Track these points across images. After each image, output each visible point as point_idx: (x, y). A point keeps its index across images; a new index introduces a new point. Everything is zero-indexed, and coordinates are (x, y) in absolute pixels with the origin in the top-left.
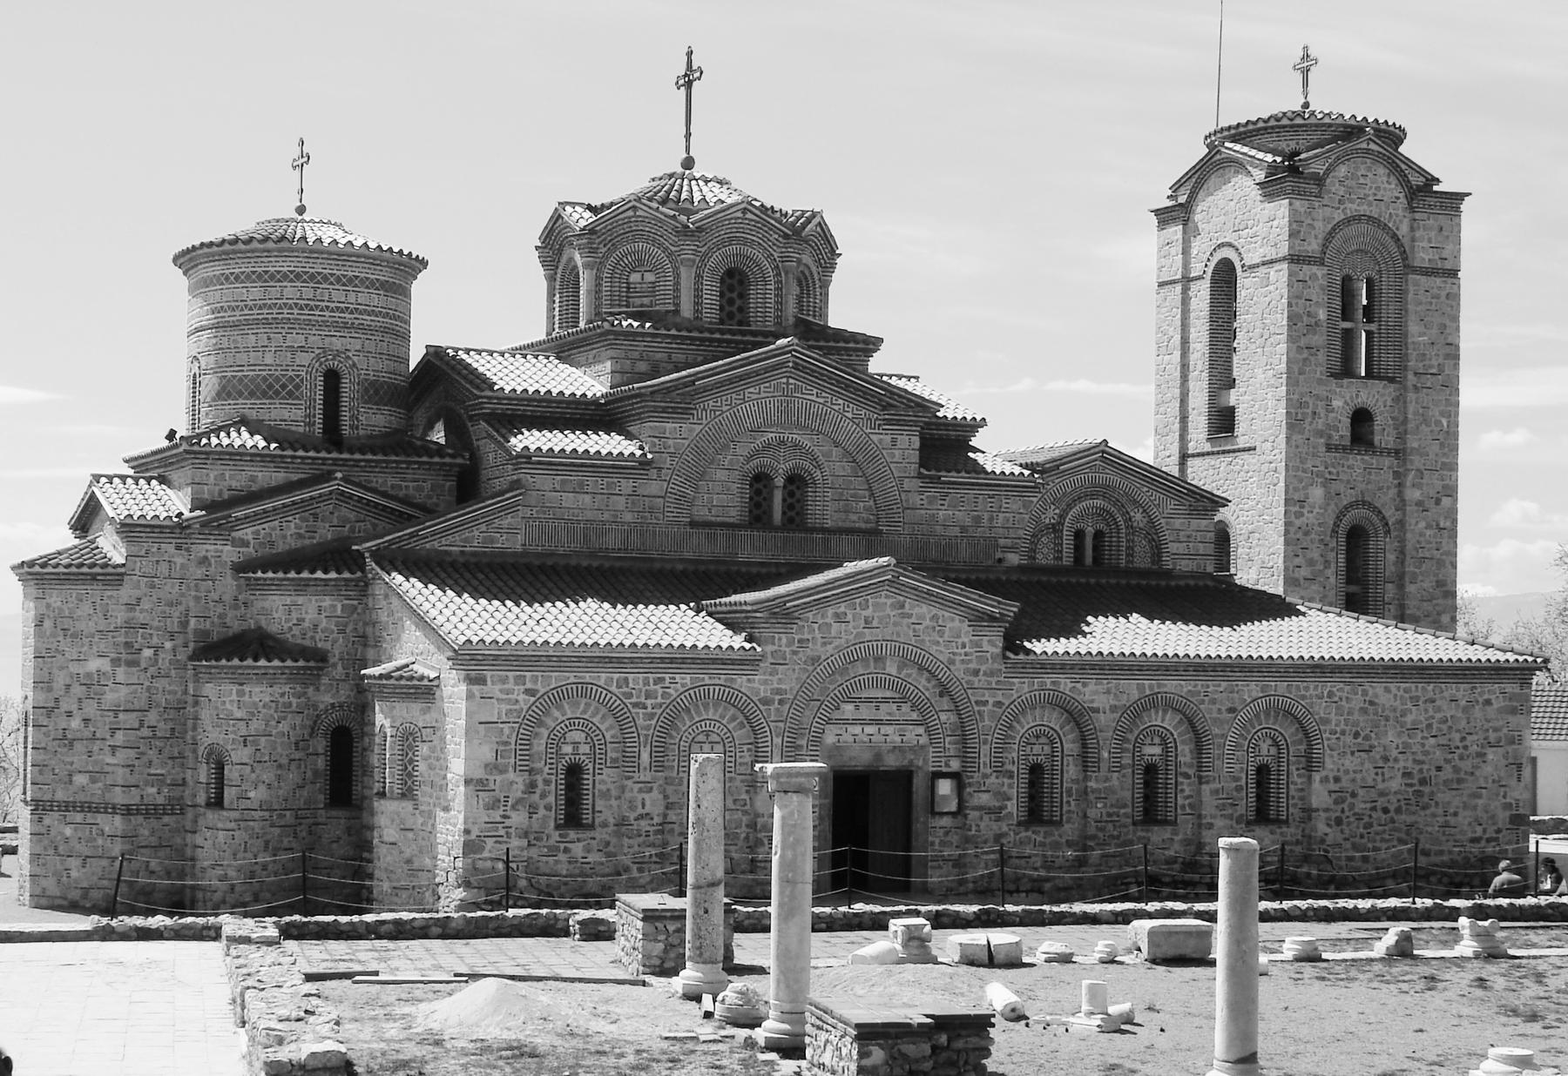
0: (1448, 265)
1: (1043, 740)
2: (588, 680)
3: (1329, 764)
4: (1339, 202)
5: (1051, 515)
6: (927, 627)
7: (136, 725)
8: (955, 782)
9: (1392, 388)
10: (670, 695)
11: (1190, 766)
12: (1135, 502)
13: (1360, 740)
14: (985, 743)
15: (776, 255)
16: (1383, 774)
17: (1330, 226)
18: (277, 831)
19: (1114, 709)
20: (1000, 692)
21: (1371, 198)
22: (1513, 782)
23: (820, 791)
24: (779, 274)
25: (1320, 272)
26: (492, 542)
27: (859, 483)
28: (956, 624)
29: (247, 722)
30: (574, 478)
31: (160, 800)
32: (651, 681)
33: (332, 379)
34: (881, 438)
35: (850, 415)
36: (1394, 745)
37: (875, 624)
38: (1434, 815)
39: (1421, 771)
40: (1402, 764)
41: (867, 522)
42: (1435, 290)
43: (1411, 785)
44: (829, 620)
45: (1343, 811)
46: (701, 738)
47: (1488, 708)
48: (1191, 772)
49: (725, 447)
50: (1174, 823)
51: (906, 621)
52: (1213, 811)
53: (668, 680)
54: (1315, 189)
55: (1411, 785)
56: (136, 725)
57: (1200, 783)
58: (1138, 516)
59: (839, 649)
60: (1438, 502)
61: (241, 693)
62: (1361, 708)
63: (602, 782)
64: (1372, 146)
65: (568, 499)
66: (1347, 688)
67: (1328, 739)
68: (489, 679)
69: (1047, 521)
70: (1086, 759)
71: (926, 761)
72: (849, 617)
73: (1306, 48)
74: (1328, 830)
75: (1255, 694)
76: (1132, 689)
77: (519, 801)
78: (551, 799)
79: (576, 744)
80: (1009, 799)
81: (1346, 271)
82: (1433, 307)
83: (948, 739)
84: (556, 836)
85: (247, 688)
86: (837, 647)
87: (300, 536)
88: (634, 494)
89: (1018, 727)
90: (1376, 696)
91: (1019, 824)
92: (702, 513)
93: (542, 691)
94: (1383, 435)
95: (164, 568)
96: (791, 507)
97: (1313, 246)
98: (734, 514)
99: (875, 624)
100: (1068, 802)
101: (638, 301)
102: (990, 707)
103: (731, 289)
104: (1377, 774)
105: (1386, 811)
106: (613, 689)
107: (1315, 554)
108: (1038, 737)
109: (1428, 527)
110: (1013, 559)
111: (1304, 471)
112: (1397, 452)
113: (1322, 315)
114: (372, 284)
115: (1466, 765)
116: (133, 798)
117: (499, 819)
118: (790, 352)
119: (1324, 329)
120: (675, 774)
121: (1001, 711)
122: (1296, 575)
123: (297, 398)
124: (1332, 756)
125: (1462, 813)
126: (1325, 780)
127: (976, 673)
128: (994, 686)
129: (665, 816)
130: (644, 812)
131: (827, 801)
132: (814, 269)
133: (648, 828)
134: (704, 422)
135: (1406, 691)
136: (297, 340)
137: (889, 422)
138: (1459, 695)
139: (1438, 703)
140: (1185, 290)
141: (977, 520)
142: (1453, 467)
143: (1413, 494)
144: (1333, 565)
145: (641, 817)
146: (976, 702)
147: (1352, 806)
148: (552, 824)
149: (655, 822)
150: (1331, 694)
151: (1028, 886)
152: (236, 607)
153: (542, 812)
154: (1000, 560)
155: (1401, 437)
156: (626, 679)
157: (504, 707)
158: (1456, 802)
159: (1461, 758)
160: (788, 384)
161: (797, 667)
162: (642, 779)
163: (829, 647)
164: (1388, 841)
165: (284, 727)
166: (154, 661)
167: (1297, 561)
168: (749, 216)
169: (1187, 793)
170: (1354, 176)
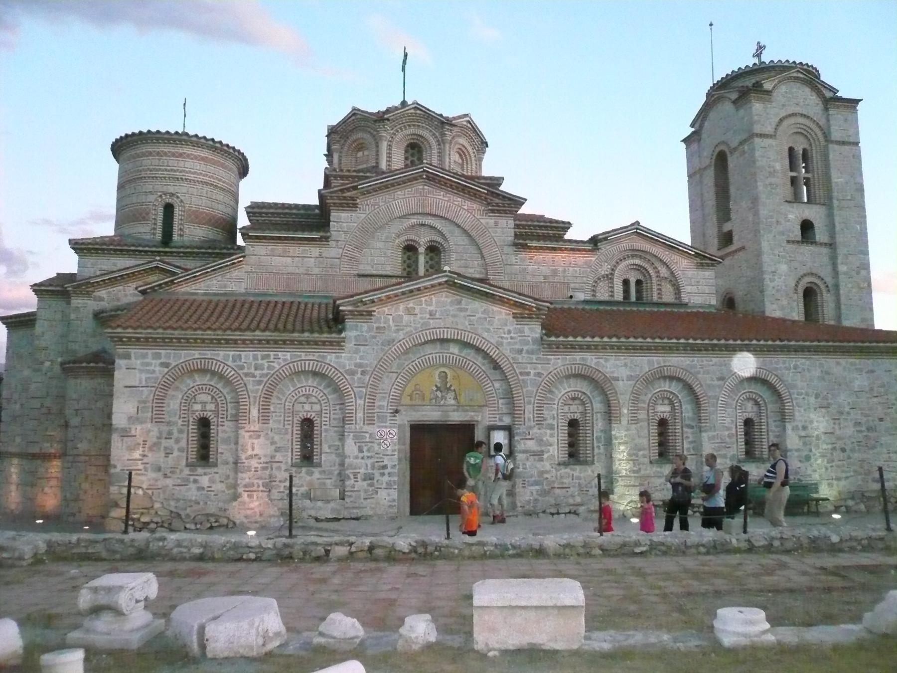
0: (852, 140)
1: (577, 402)
2: (209, 357)
5: (605, 269)
6: (480, 318)
8: (507, 433)
10: (274, 367)
11: (693, 419)
14: (529, 403)
15: (437, 134)
16: (839, 424)
19: (630, 378)
20: (539, 366)
23: (399, 439)
26: (225, 287)
30: (279, 247)
32: (259, 357)
33: (169, 209)
34: (489, 221)
35: (466, 207)
36: (846, 402)
37: (437, 316)
39: (868, 421)
46: (303, 399)
48: (693, 424)
51: (462, 314)
53: (272, 357)
56: (39, 406)
57: (701, 431)
58: (664, 271)
59: (410, 334)
60: (858, 273)
63: (224, 431)
65: (277, 261)
66: (808, 362)
67: (796, 399)
68: (133, 355)
69: (603, 273)
72: (417, 311)
73: (759, 43)
74: (799, 465)
77: (155, 444)
78: (183, 443)
79: (204, 403)
80: (551, 445)
84: (187, 471)
85: (79, 381)
86: (407, 333)
88: (320, 256)
89: (556, 392)
91: (559, 464)
93: (174, 364)
94: (820, 235)
99: (437, 316)
100: (598, 447)
102: (532, 376)
105: (843, 450)
106: (230, 363)
108: (574, 399)
110: (581, 296)
112: (831, 245)
113: (778, 166)
118: (422, 168)
120: (281, 426)
121: (541, 379)
123: (147, 220)
124: (800, 411)
127: (520, 351)
130: (255, 452)
132: (470, 149)
133: (257, 465)
134: (368, 212)
137: (493, 211)
140: (701, 176)
142: (866, 253)
143: (842, 268)
144: (796, 309)
145: (251, 457)
146: (521, 373)
149: (261, 461)
150: (795, 367)
153: (176, 453)
155: (832, 235)
156: (240, 355)
157: (144, 376)
160: (423, 189)
161: (375, 348)
162: (252, 428)
163: (401, 333)
164: (846, 472)
169: (691, 439)
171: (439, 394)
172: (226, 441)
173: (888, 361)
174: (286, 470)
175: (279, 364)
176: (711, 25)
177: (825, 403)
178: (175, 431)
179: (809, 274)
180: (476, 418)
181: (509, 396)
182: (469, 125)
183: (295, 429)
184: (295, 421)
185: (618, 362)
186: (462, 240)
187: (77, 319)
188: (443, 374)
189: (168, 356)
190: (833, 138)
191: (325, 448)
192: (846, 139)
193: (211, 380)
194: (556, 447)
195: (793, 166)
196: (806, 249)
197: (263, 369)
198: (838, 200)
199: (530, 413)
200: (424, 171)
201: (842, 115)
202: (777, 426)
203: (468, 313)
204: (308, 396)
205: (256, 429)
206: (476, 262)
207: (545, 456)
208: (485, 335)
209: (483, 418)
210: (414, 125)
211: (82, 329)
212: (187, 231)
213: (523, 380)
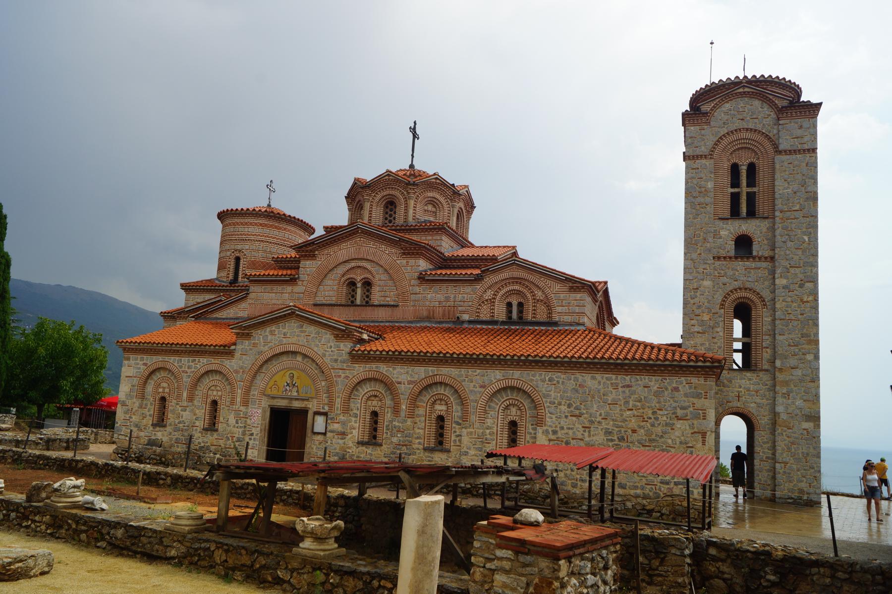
1: (377, 399)
4: (724, 123)
5: (489, 295)
6: (313, 337)
13: (572, 409)
16: (589, 432)
19: (410, 383)
20: (348, 371)
22: (700, 445)
24: (406, 201)
27: (390, 283)
28: (327, 336)
30: (268, 287)
33: (238, 259)
35: (387, 252)
36: (598, 413)
40: (604, 425)
43: (612, 440)
44: (266, 334)
46: (213, 388)
47: (676, 394)
51: (303, 334)
53: (197, 361)
55: (612, 440)
58: (539, 294)
60: (801, 286)
62: (574, 389)
64: (747, 90)
67: (549, 407)
69: (487, 298)
70: (396, 411)
72: (276, 333)
76: (421, 372)
77: (136, 411)
78: (152, 412)
79: (164, 388)
80: (354, 429)
84: (151, 428)
89: (361, 391)
90: (585, 381)
91: (358, 443)
92: (320, 299)
96: (353, 296)
97: (704, 150)
98: (333, 300)
100: (387, 433)
103: (391, 210)
104: (584, 431)
106: (176, 364)
107: (706, 317)
108: (376, 396)
110: (466, 317)
113: (710, 185)
117: (128, 418)
118: (356, 225)
119: (712, 195)
126: (547, 431)
127: (336, 361)
128: (345, 368)
130: (183, 420)
131: (264, 422)
135: (607, 379)
137: (404, 254)
138: (652, 384)
141: (447, 299)
142: (815, 265)
143: (780, 282)
144: (721, 324)
148: (151, 423)
149: (186, 425)
150: (550, 380)
159: (653, 425)
162: (183, 405)
163: (266, 347)
168: (391, 178)
169: (458, 433)
171: (288, 388)
173: (647, 377)
174: (200, 432)
175: (200, 365)
176: (712, 43)
177: (577, 412)
178: (149, 404)
180: (308, 406)
181: (329, 391)
183: (207, 406)
184: (208, 402)
185: (402, 371)
186: (384, 277)
188: (292, 375)
190: (781, 147)
191: (221, 419)
192: (800, 147)
193: (168, 374)
194: (357, 430)
195: (735, 183)
196: (740, 265)
197: (192, 368)
198: (781, 212)
199: (338, 404)
200: (358, 228)
201: (795, 122)
202: (533, 429)
203: (307, 334)
204: (216, 386)
205: (185, 405)
206: (392, 293)
208: (316, 349)
209: (313, 406)
210: (389, 188)
213: (336, 381)
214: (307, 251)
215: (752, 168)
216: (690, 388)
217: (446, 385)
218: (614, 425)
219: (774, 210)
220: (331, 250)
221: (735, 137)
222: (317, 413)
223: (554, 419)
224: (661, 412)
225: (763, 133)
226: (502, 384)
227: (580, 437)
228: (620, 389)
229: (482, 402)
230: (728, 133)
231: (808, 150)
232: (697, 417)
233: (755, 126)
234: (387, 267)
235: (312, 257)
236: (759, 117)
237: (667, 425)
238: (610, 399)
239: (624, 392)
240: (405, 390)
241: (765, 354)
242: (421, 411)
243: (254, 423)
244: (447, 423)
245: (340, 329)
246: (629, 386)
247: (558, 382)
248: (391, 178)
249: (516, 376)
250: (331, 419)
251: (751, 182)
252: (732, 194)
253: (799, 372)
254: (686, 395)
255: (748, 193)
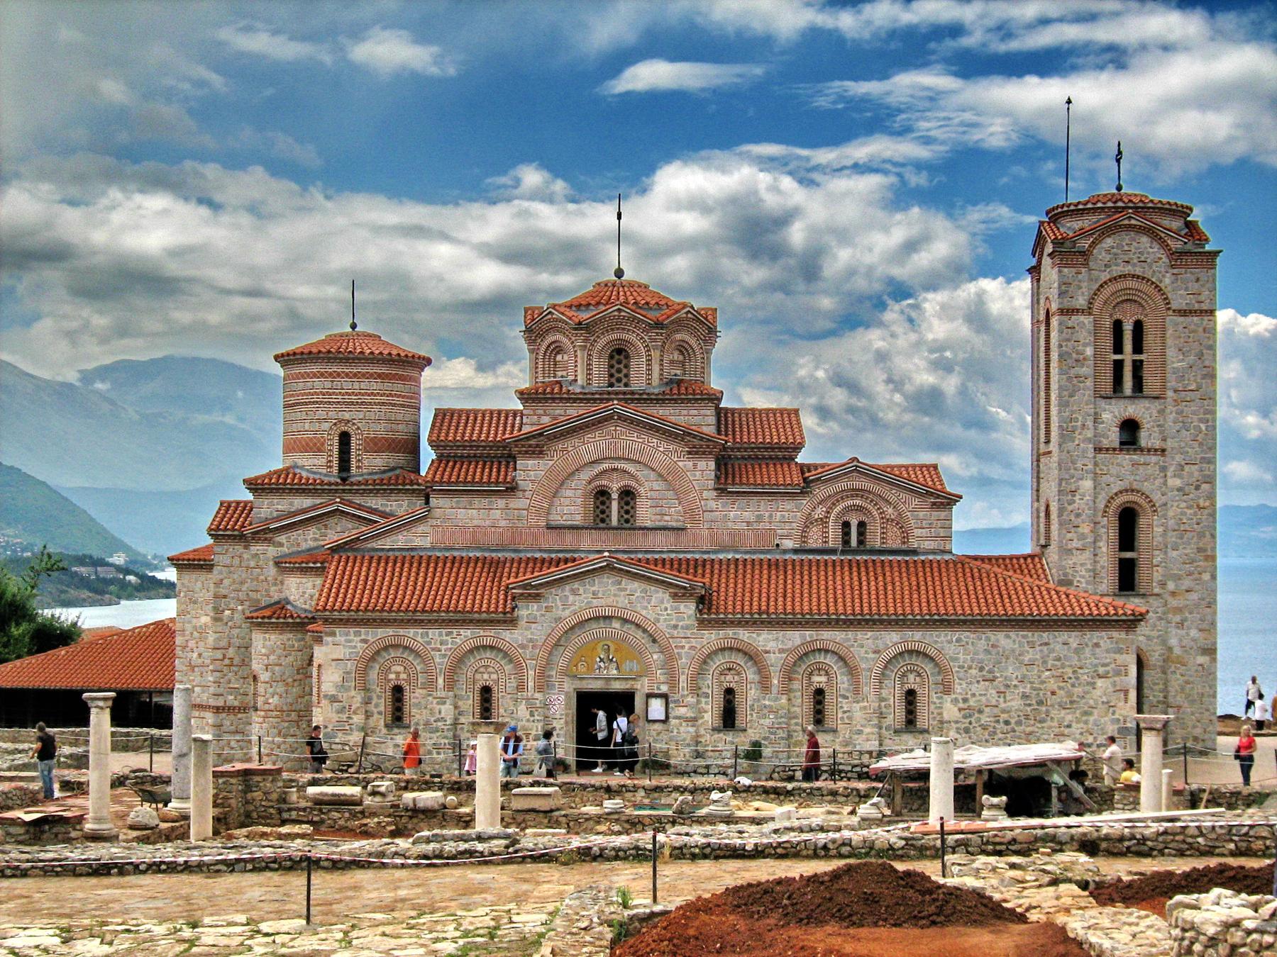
0: (1205, 307)
1: (732, 672)
3: (958, 689)
5: (819, 512)
7: (221, 657)
8: (664, 700)
9: (1157, 403)
11: (848, 690)
12: (887, 501)
13: (984, 673)
14: (683, 673)
16: (1005, 697)
17: (1097, 286)
18: (286, 724)
19: (781, 651)
21: (1135, 261)
22: (1121, 704)
23: (566, 704)
25: (1087, 320)
28: (660, 596)
29: (268, 656)
30: (464, 500)
31: (236, 703)
33: (345, 439)
35: (661, 449)
36: (1014, 676)
37: (600, 596)
38: (1050, 727)
41: (678, 521)
42: (1193, 327)
43: (1030, 705)
45: (970, 723)
46: (482, 670)
47: (1098, 650)
49: (573, 473)
50: (835, 731)
52: (864, 722)
54: (1081, 260)
55: (1030, 705)
56: (221, 657)
60: (1197, 488)
61: (265, 639)
64: (1133, 222)
66: (972, 636)
67: (957, 672)
70: (765, 686)
71: (642, 686)
72: (581, 591)
74: (958, 736)
75: (895, 640)
76: (795, 638)
77: (358, 708)
78: (382, 708)
79: (398, 673)
80: (706, 712)
81: (1117, 316)
82: (1191, 340)
83: (659, 672)
84: (384, 731)
85: (267, 636)
87: (316, 539)
90: (998, 640)
91: (714, 729)
92: (557, 519)
95: (236, 561)
98: (578, 520)
100: (752, 715)
101: (559, 374)
102: (686, 650)
103: (619, 362)
105: (1007, 723)
106: (419, 639)
107: (1085, 529)
108: (730, 669)
109: (1189, 507)
110: (788, 544)
111: (1075, 469)
112: (1163, 451)
113: (1089, 351)
114: (371, 376)
115: (1078, 690)
116: (220, 703)
122: (1069, 547)
125: (1074, 725)
126: (956, 700)
127: (675, 627)
129: (456, 719)
131: (570, 712)
135: (1023, 637)
136: (321, 414)
137: (689, 453)
138: (1071, 640)
139: (1052, 646)
141: (759, 519)
144: (1105, 537)
147: (979, 720)
148: (382, 722)
150: (958, 640)
151: (716, 771)
152: (275, 584)
153: (376, 716)
154: (778, 545)
156: (427, 633)
158: (1069, 717)
159: (1073, 686)
162: (439, 695)
165: (291, 659)
166: (231, 619)
167: (1069, 536)
168: (623, 314)
170: (1119, 246)
171: (602, 664)
172: (418, 705)
177: (990, 676)
179: (1127, 491)
180: (635, 687)
182: (689, 315)
185: (770, 637)
187: (258, 567)
189: (367, 634)
191: (502, 711)
192: (1197, 306)
193: (403, 653)
196: (1125, 459)
198: (1175, 391)
201: (1191, 273)
202: (937, 698)
203: (628, 592)
204: (486, 667)
207: (700, 721)
208: (644, 612)
209: (642, 687)
211: (262, 577)
212: (366, 462)
214: (530, 446)
215: (1138, 327)
216: (1112, 642)
217: (827, 651)
218: (1032, 688)
219: (1164, 387)
220: (570, 444)
221: (1119, 286)
222: (650, 696)
223: (964, 686)
224: (1081, 671)
225: (1153, 283)
226: (901, 648)
227: (994, 702)
228: (1038, 648)
229: (877, 669)
230: (1110, 280)
231: (1206, 311)
232: (1118, 673)
233: (1144, 272)
234: (664, 472)
235: (538, 452)
236: (1149, 260)
237: (1088, 683)
238: (1026, 659)
239: (1041, 651)
240: (775, 661)
241: (1155, 574)
242: (796, 685)
243: (554, 714)
244: (829, 698)
245: (677, 586)
246: (1046, 644)
247: (967, 643)
248: (623, 314)
249: (916, 637)
250: (675, 702)
251: (1138, 348)
252: (1115, 361)
253: (1194, 596)
254: (1108, 651)
255: (1134, 362)
